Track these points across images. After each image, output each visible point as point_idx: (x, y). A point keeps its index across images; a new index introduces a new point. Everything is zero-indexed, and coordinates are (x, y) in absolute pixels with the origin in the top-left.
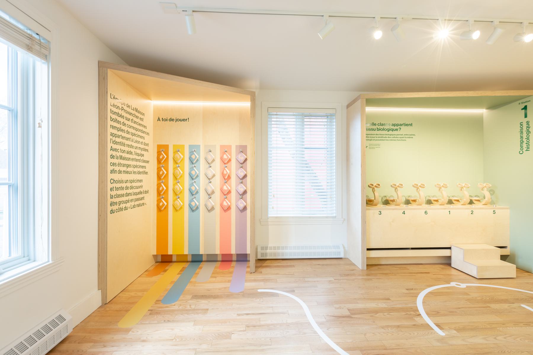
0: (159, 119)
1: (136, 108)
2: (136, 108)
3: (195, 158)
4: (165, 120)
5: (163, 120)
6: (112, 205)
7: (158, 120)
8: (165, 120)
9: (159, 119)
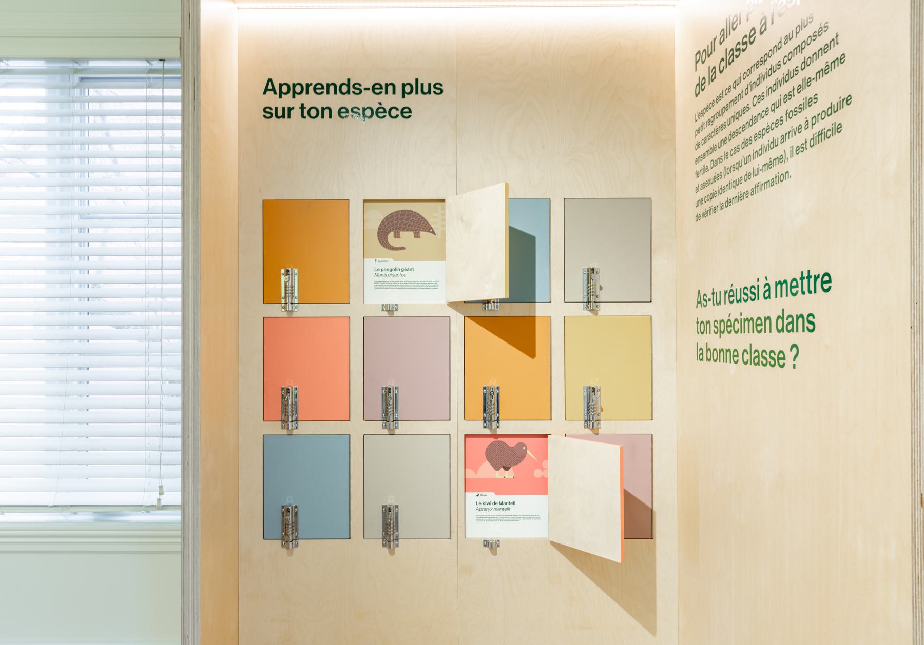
0: (270, 87)
1: (835, 41)
2: (835, 41)
3: (733, 359)
4: (313, 113)
5: (306, 111)
6: (799, 289)
7: (266, 90)
8: (313, 113)
9: (270, 87)
